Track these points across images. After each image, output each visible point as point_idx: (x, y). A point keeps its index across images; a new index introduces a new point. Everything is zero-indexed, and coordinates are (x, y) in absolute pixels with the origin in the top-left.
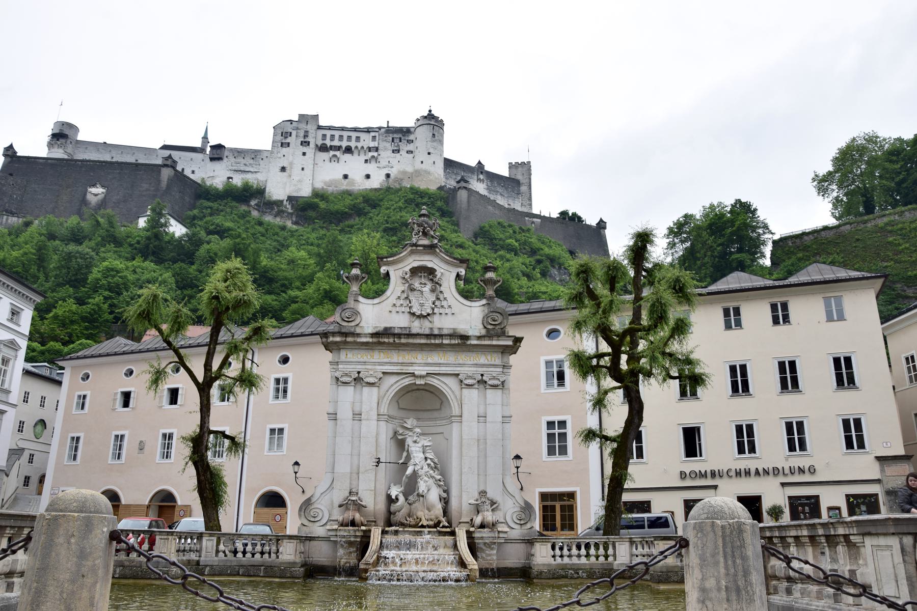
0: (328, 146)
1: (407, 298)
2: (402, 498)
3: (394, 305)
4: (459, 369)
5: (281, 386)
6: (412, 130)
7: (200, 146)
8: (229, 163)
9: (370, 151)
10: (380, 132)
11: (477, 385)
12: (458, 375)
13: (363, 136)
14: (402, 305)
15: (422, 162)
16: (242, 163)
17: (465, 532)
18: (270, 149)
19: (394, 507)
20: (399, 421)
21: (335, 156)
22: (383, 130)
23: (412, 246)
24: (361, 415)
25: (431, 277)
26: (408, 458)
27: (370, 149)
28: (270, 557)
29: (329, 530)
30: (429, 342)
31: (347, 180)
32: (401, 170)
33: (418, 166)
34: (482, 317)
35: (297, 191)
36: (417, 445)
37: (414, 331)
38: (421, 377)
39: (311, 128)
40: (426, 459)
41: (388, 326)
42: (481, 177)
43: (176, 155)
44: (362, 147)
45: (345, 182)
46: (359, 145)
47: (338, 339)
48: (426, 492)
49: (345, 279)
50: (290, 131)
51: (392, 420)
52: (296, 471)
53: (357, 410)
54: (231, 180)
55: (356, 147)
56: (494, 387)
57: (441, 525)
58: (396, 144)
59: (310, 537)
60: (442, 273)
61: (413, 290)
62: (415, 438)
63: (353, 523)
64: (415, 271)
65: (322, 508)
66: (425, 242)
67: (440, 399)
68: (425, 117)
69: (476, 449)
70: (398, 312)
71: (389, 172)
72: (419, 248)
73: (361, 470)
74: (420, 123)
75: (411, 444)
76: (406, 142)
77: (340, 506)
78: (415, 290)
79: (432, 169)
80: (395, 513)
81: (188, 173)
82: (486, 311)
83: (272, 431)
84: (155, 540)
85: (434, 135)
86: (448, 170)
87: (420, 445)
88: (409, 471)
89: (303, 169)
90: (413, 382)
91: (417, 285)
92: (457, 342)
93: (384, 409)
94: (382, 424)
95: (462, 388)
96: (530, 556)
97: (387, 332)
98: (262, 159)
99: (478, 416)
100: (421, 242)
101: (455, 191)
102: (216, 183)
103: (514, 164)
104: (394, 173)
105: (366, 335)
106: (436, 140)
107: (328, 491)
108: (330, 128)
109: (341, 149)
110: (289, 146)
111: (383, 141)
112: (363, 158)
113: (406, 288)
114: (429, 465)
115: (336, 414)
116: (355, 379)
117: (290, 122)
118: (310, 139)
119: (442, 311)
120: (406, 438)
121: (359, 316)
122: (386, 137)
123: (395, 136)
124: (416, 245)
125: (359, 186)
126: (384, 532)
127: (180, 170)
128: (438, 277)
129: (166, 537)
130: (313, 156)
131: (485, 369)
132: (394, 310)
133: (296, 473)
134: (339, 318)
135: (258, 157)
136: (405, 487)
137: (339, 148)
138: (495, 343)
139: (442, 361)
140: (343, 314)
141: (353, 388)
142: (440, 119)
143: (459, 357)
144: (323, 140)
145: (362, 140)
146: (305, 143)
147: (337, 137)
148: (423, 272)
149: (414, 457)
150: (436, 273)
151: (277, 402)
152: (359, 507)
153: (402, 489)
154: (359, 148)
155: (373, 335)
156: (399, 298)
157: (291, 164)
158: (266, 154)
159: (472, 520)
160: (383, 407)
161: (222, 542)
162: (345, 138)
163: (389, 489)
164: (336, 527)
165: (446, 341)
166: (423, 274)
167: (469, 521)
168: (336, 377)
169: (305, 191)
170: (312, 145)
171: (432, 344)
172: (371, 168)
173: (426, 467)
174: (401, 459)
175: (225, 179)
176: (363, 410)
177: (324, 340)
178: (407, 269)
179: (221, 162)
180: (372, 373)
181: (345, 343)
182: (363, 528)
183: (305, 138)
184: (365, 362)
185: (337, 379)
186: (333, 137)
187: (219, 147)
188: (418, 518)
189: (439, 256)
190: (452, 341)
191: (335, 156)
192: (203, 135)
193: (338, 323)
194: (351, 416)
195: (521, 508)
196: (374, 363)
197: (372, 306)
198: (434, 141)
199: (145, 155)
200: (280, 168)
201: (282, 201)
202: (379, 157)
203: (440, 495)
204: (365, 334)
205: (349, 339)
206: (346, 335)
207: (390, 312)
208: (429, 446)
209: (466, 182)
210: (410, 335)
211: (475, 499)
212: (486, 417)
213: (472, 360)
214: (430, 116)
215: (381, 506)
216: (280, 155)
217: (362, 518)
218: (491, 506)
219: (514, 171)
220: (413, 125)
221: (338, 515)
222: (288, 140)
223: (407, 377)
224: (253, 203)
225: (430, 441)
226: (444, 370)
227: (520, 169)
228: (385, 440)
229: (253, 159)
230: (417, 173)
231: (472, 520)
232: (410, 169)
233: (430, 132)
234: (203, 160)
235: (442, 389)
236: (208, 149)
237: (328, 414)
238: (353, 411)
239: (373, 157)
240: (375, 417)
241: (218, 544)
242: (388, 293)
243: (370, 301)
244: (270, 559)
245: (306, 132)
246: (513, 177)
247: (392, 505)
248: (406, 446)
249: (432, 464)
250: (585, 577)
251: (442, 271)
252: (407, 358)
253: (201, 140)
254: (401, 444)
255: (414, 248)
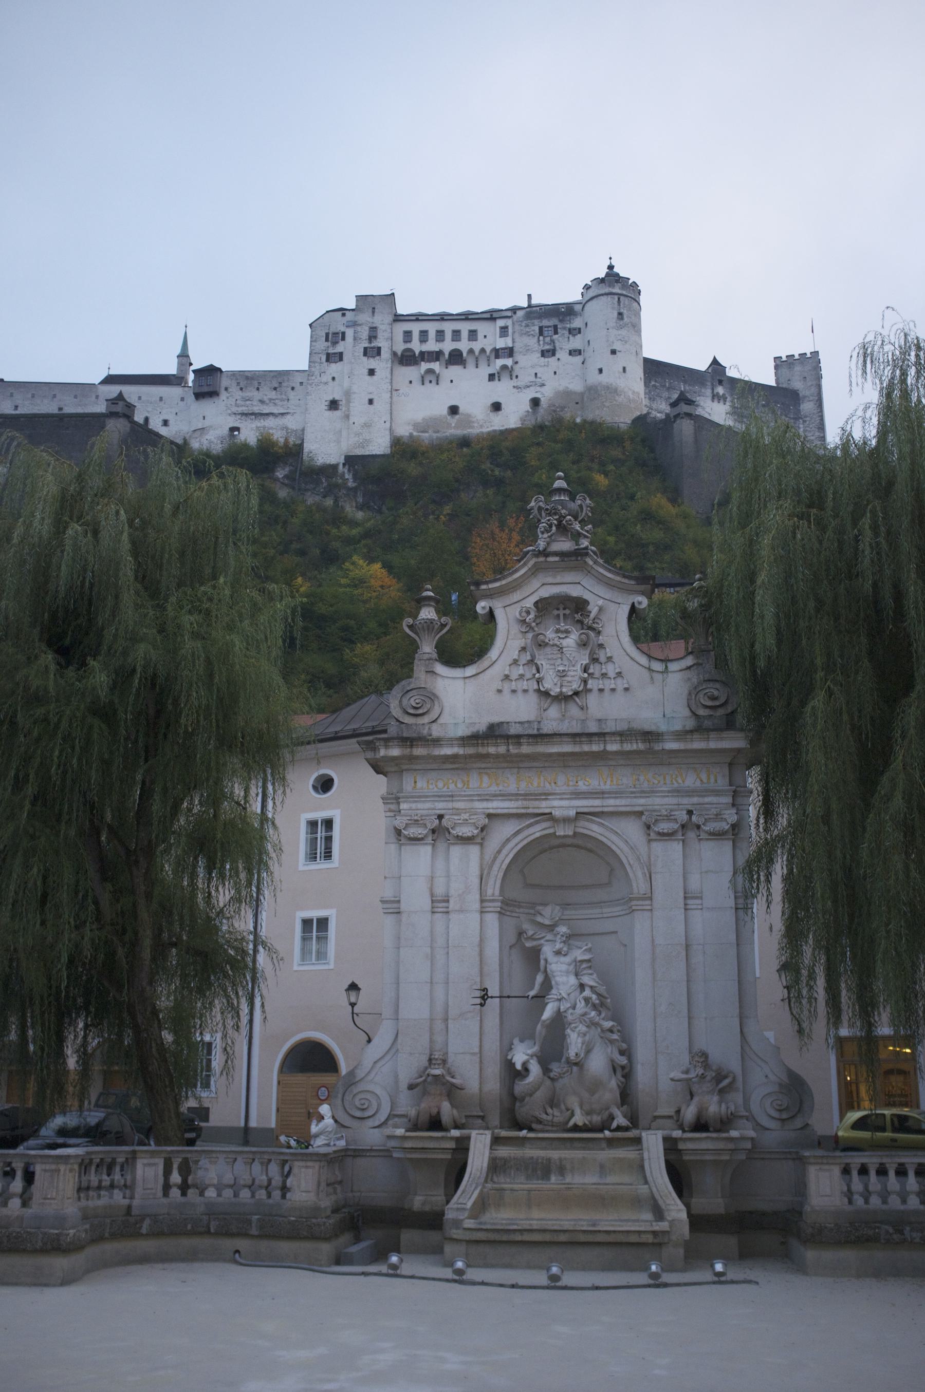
0: (417, 353)
1: (531, 661)
2: (535, 1069)
3: (507, 677)
4: (642, 801)
5: (321, 833)
6: (578, 308)
7: (175, 373)
8: (232, 401)
9: (497, 357)
10: (515, 317)
11: (680, 833)
12: (640, 814)
13: (482, 328)
14: (521, 676)
15: (601, 371)
16: (255, 399)
17: (660, 1140)
18: (307, 368)
19: (520, 1087)
20: (527, 911)
21: (430, 371)
22: (520, 314)
23: (537, 556)
24: (448, 901)
25: (578, 616)
26: (547, 985)
27: (497, 353)
28: (269, 1196)
29: (390, 1137)
30: (577, 749)
31: (457, 417)
32: (561, 388)
33: (594, 378)
34: (686, 692)
35: (362, 445)
36: (562, 959)
37: (547, 728)
38: (566, 820)
39: (382, 320)
40: (582, 987)
41: (496, 719)
42: (720, 390)
43: (131, 392)
44: (483, 351)
45: (453, 420)
46: (477, 346)
47: (395, 752)
48: (582, 1055)
49: (407, 630)
50: (343, 329)
51: (511, 908)
52: (353, 1000)
53: (440, 891)
54: (236, 433)
55: (471, 351)
56: (717, 835)
57: (614, 1125)
58: (548, 339)
59: (355, 1150)
60: (601, 609)
61: (542, 645)
62: (558, 946)
63: (435, 1124)
64: (544, 607)
65: (379, 1091)
66: (565, 545)
67: (608, 863)
68: (602, 281)
69: (683, 965)
70: (514, 691)
71: (538, 395)
72: (551, 559)
73: (452, 1013)
74: (591, 293)
75: (551, 958)
76: (566, 333)
77: (411, 1087)
78: (547, 644)
79: (621, 383)
80: (522, 1099)
81: (155, 425)
82: (695, 680)
83: (307, 923)
84: (33, 1173)
85: (620, 314)
86: (653, 383)
87: (567, 959)
88: (548, 1013)
89: (371, 402)
90: (551, 831)
91: (550, 634)
92: (635, 747)
93: (493, 889)
94: (492, 920)
95: (650, 841)
96: (801, 1188)
97: (494, 733)
98: (293, 389)
99: (685, 898)
100: (557, 547)
101: (669, 421)
102: (210, 442)
103: (784, 359)
104: (546, 394)
105: (451, 741)
106: (626, 325)
107: (387, 1058)
108: (418, 318)
109: (441, 358)
110: (341, 359)
111: (521, 335)
112: (485, 371)
113: (529, 641)
114: (587, 1000)
115: (399, 902)
116: (433, 831)
117: (340, 313)
118: (382, 342)
119: (600, 684)
120: (541, 945)
121: (436, 703)
122: (527, 326)
123: (545, 322)
124: (545, 553)
125: (481, 426)
126: (496, 1141)
127: (141, 421)
128: (592, 615)
129: (53, 1167)
130: (389, 376)
131: (695, 800)
132: (507, 687)
133: (353, 1005)
134: (398, 709)
135: (284, 384)
136: (542, 1049)
137: (436, 356)
138: (713, 745)
139: (607, 787)
140: (405, 701)
141: (429, 849)
142: (630, 282)
143: (642, 778)
144: (405, 342)
145: (480, 336)
146: (372, 352)
147: (432, 335)
148: (561, 607)
149: (557, 984)
150: (589, 608)
151: (314, 866)
152: (452, 1091)
153: (536, 1049)
154: (477, 353)
155: (466, 740)
156: (515, 662)
157: (348, 394)
158: (299, 378)
159: (678, 1112)
160: (491, 882)
161: (175, 1166)
162: (448, 335)
163: (511, 1049)
164: (400, 1132)
165: (613, 747)
166: (561, 612)
167: (673, 1114)
168: (395, 828)
169: (380, 445)
170: (386, 354)
171: (586, 753)
172: (502, 390)
173: (581, 1005)
174: (532, 988)
175: (225, 431)
176: (452, 892)
177: (370, 755)
178: (529, 603)
179: (215, 399)
180: (466, 816)
181: (412, 759)
182: (455, 1133)
183: (370, 342)
184: (452, 796)
185: (398, 832)
186: (424, 335)
187: (210, 372)
188: (568, 1110)
189: (593, 572)
190: (625, 745)
191: (430, 371)
192: (178, 351)
193: (398, 720)
194: (426, 903)
195: (780, 1085)
196: (470, 798)
197: (461, 682)
198: (621, 327)
199: (76, 397)
200: (327, 403)
201: (334, 467)
202: (516, 367)
203: (612, 1061)
204: (451, 739)
205: (419, 751)
206: (409, 741)
207: (499, 691)
208: (589, 961)
209: (690, 402)
210: (540, 737)
211: (684, 1068)
212: (701, 898)
213: (668, 781)
214: (612, 277)
215: (494, 1085)
216: (327, 378)
217: (455, 1112)
218: (717, 1084)
219: (784, 371)
220: (579, 298)
221: (407, 1105)
222: (339, 348)
223: (537, 823)
224: (280, 474)
225: (589, 950)
226: (611, 804)
227: (798, 368)
228: (498, 949)
229: (275, 389)
230: (593, 391)
231: (678, 1112)
232: (577, 386)
233: (613, 308)
234: (182, 399)
235: (609, 844)
236: (191, 377)
237: (383, 902)
238: (432, 895)
239: (504, 367)
240: (477, 906)
241: (167, 1172)
242: (494, 653)
243: (458, 672)
244: (271, 1201)
245: (373, 329)
246: (784, 386)
247: (516, 1081)
248: (542, 962)
249: (594, 997)
250: (917, 1240)
251: (600, 602)
252: (535, 784)
253: (176, 360)
254: (533, 957)
255: (542, 559)
